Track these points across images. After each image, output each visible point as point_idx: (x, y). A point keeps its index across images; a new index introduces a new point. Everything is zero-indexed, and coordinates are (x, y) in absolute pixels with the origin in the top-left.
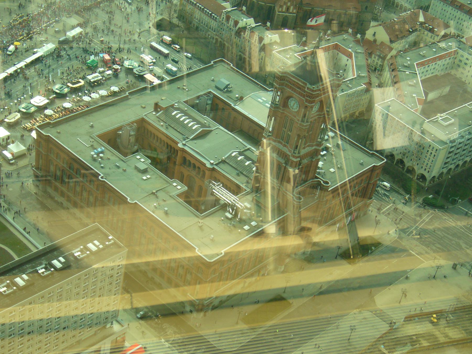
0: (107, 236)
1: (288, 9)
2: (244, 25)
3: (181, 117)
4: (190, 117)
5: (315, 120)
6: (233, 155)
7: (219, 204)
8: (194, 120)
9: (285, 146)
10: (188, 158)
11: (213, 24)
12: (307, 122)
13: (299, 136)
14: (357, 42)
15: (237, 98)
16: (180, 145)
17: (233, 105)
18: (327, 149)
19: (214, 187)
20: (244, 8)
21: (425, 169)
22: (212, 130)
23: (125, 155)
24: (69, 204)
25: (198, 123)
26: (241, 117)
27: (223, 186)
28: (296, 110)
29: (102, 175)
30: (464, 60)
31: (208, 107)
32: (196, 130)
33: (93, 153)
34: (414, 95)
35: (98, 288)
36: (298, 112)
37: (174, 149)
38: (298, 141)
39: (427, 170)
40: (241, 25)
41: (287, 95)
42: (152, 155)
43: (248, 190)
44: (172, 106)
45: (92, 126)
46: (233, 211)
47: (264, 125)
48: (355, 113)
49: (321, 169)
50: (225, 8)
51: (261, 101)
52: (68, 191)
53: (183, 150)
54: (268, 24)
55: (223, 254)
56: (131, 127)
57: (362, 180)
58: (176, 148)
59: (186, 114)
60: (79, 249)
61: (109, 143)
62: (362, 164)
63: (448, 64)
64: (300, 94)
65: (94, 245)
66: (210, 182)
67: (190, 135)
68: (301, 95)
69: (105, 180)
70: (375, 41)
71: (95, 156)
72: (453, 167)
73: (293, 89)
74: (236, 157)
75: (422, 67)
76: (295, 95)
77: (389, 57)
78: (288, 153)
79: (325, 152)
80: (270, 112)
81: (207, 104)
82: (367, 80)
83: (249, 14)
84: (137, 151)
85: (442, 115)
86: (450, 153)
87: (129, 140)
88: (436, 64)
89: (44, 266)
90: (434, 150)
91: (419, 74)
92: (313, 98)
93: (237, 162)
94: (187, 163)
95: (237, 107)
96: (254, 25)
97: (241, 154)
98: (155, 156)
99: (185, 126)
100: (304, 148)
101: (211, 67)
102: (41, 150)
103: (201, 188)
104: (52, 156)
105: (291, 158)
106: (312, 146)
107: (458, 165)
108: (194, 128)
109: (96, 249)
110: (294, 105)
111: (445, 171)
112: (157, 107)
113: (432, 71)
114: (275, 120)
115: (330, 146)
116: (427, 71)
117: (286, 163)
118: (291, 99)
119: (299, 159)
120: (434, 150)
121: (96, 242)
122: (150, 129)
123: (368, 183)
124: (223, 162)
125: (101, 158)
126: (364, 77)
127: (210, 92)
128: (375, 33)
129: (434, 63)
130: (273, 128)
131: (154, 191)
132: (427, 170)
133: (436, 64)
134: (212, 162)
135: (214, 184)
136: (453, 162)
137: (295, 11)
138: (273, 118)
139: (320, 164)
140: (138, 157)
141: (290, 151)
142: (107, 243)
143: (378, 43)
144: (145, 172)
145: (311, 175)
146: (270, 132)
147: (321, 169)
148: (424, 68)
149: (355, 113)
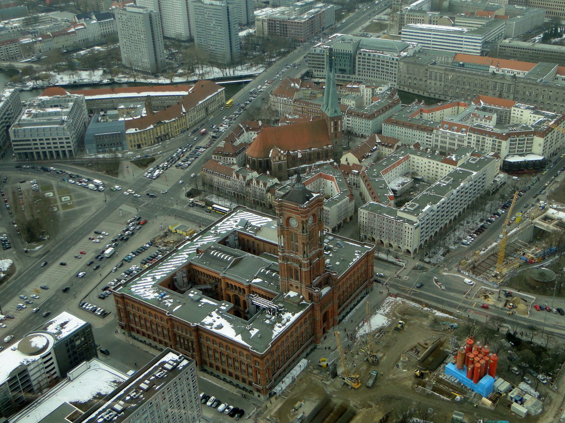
1: (280, 158)
3: (217, 254)
4: (224, 252)
7: (259, 309)
8: (227, 253)
9: (296, 254)
10: (230, 282)
11: (228, 182)
12: (306, 232)
13: (303, 244)
16: (222, 275)
18: (329, 249)
20: (248, 166)
23: (182, 292)
24: (150, 340)
25: (231, 255)
26: (262, 243)
27: (260, 296)
30: (416, 160)
31: (237, 242)
32: (231, 260)
35: (181, 396)
36: (298, 227)
38: (304, 248)
40: (248, 178)
41: (286, 217)
43: (279, 294)
46: (270, 312)
47: (277, 243)
48: (346, 219)
49: (330, 264)
50: (234, 170)
51: (274, 227)
52: (147, 331)
53: (224, 278)
54: (268, 172)
56: (182, 271)
59: (221, 251)
60: (158, 371)
61: (169, 287)
64: (295, 213)
66: (249, 296)
68: (297, 214)
70: (348, 164)
71: (160, 299)
72: (428, 238)
73: (290, 212)
74: (264, 272)
76: (293, 215)
77: (361, 172)
78: (300, 258)
79: (329, 252)
81: (235, 240)
82: (349, 193)
83: (253, 168)
84: (191, 287)
87: (183, 281)
89: (134, 390)
90: (410, 229)
94: (230, 286)
95: (257, 237)
96: (258, 175)
97: (267, 269)
100: (311, 252)
102: (120, 306)
103: (245, 302)
104: (129, 308)
105: (303, 261)
106: (316, 249)
107: (431, 236)
110: (294, 223)
111: (423, 242)
114: (284, 237)
115: (332, 246)
117: (300, 267)
120: (410, 229)
122: (197, 268)
130: (284, 243)
134: (248, 280)
135: (252, 297)
137: (285, 159)
139: (328, 261)
141: (301, 257)
143: (351, 165)
145: (322, 270)
147: (330, 264)
149: (346, 219)
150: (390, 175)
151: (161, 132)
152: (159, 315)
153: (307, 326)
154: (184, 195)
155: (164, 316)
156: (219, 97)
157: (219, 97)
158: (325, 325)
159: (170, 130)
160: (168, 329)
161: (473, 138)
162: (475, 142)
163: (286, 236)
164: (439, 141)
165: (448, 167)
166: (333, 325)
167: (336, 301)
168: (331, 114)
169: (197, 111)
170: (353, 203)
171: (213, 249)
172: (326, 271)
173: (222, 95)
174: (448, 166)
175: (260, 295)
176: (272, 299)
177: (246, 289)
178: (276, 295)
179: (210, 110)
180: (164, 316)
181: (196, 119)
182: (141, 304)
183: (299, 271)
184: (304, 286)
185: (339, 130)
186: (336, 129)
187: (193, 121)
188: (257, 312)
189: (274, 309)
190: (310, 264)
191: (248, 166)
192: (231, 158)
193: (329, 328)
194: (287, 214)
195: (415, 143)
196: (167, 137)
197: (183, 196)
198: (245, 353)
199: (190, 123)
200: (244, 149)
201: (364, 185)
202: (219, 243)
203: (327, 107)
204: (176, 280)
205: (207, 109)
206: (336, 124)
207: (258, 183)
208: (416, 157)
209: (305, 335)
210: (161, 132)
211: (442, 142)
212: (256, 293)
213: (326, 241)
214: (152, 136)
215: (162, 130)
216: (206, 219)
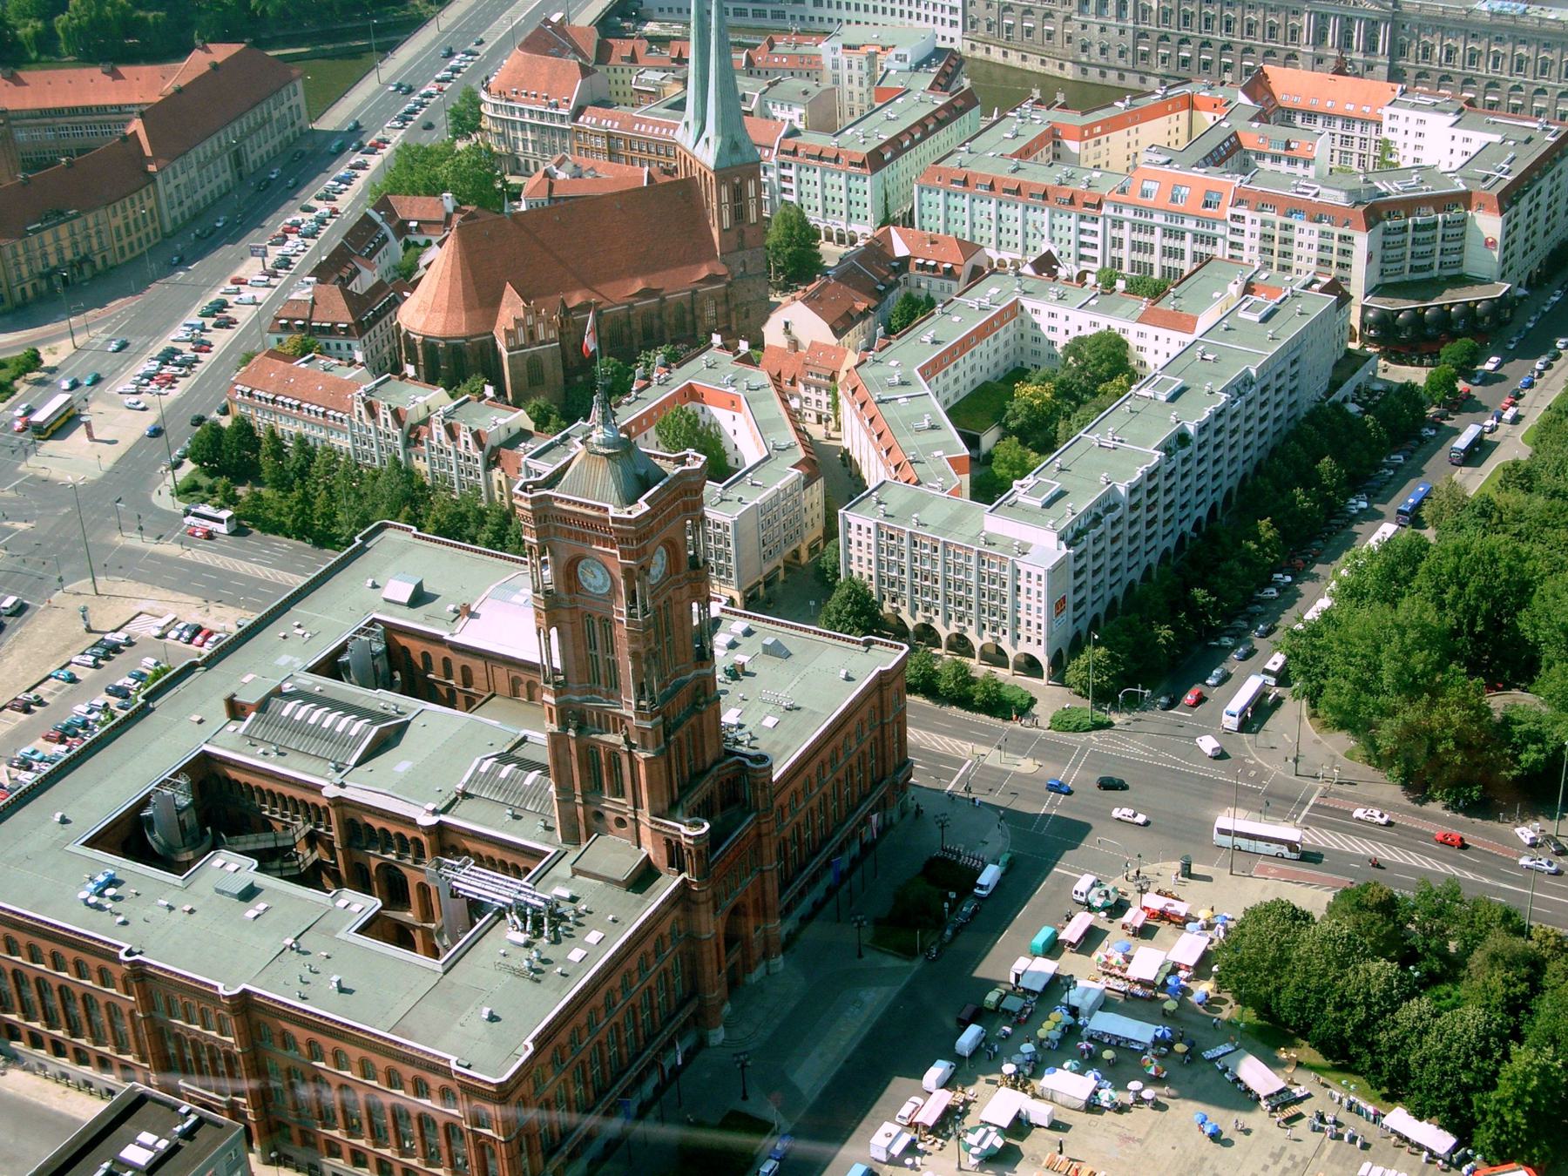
0: (175, 1108)
1: (532, 335)
2: (422, 414)
3: (309, 714)
4: (334, 705)
5: (670, 598)
6: (484, 769)
8: (348, 709)
14: (747, 360)
15: (456, 611)
16: (331, 791)
17: (447, 637)
18: (736, 673)
19: (452, 875)
21: (1029, 639)
22: (408, 723)
25: (362, 713)
28: (606, 590)
29: (127, 947)
31: (382, 665)
33: (83, 895)
34: (937, 454)
37: (315, 805)
39: (1034, 640)
41: (565, 556)
42: (261, 846)
43: (553, 851)
44: (278, 693)
45: (64, 821)
46: (525, 922)
48: (796, 554)
53: (339, 802)
55: (531, 1048)
57: (862, 722)
58: (322, 803)
59: (320, 701)
62: (848, 679)
63: (1006, 344)
65: (141, 1145)
66: (439, 865)
67: (350, 756)
69: (138, 957)
70: (795, 344)
74: (492, 773)
75: (940, 375)
77: (842, 376)
80: (538, 615)
83: (431, 378)
85: (1024, 481)
86: (1077, 574)
88: (972, 354)
91: (937, 395)
92: (639, 540)
93: (501, 787)
97: (504, 759)
98: (271, 845)
99: (329, 736)
101: (361, 551)
103: (424, 889)
108: (353, 732)
109: (152, 1154)
111: (1083, 625)
112: (235, 710)
113: (970, 376)
114: (560, 634)
116: (956, 380)
118: (583, 563)
119: (659, 718)
121: (147, 1137)
123: (883, 725)
124: (465, 795)
125: (114, 898)
126: (789, 447)
127: (374, 620)
128: (787, 324)
129: (967, 355)
131: (289, 941)
132: (1034, 640)
133: (972, 354)
134: (431, 806)
136: (1097, 595)
137: (552, 335)
138: (554, 631)
139: (729, 717)
140: (218, 862)
142: (178, 1129)
144: (249, 894)
146: (555, 672)
147: (740, 726)
148: (946, 374)
150: (950, 380)
151: (60, 251)
152: (93, 962)
153: (666, 964)
154: (166, 491)
155: (110, 966)
156: (284, 109)
157: (284, 109)
158: (736, 956)
159: (95, 241)
160: (132, 1012)
161: (1247, 227)
162: (1256, 242)
163: (567, 628)
164: (1126, 244)
165: (1162, 339)
166: (766, 955)
167: (772, 864)
168: (719, 158)
169: (202, 166)
170: (818, 489)
171: (291, 696)
172: (733, 754)
173: (294, 101)
174: (1164, 333)
175: (481, 861)
176: (528, 870)
177: (424, 839)
178: (542, 854)
179: (252, 158)
180: (110, 966)
181: (198, 197)
182: (18, 926)
183: (625, 760)
184: (645, 816)
185: (753, 218)
186: (739, 214)
187: (188, 203)
188: (473, 924)
189: (536, 910)
190: (667, 735)
191: (410, 370)
192: (344, 343)
193: (749, 969)
194: (568, 548)
195: (1038, 254)
196: (87, 268)
197: (164, 499)
198: (435, 1081)
199: (176, 212)
200: (395, 303)
201: (856, 422)
202: (314, 670)
203: (703, 129)
204: (150, 819)
205: (238, 159)
206: (738, 194)
207: (452, 432)
208: (1045, 308)
209: (659, 999)
210: (60, 251)
211: (1137, 247)
212: (467, 852)
213: (721, 640)
214: (25, 270)
215: (66, 243)
216: (263, 582)
